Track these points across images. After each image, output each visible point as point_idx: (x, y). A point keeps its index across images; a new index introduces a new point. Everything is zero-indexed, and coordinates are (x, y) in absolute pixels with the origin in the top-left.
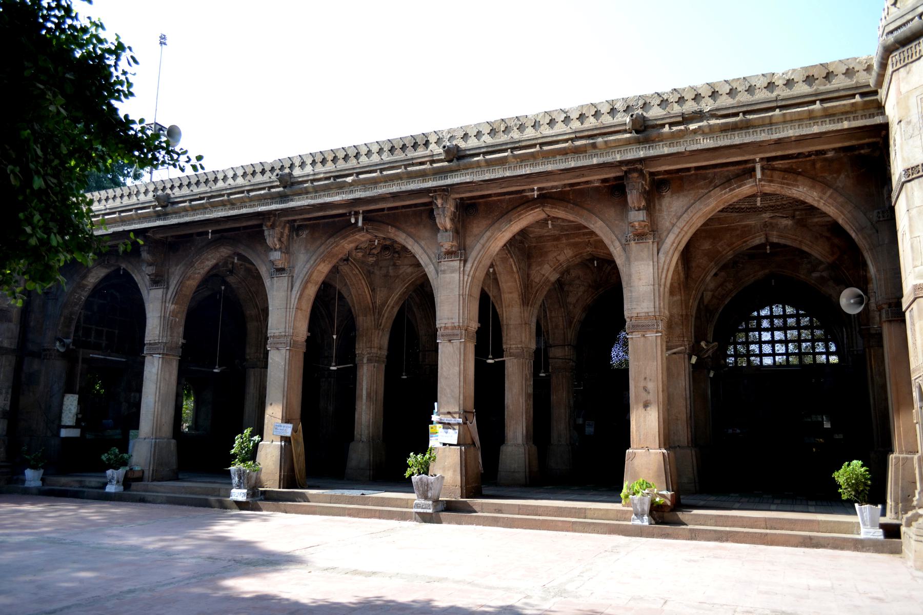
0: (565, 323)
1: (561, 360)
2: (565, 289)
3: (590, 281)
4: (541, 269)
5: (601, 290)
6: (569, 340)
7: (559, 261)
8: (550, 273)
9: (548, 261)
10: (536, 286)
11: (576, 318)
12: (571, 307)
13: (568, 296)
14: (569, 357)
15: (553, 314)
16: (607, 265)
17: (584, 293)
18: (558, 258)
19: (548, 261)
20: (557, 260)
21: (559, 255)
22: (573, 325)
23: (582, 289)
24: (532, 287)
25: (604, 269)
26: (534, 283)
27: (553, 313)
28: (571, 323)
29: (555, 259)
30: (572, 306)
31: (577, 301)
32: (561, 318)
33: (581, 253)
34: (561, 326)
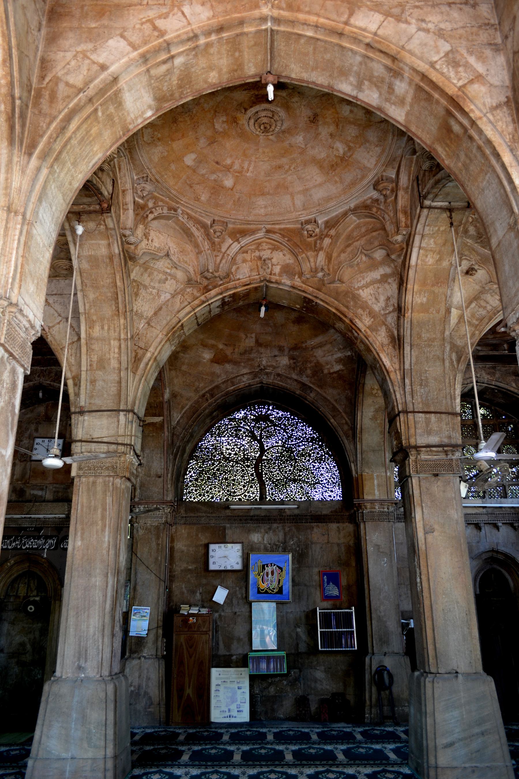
0: (124, 358)
1: (104, 448)
2: (133, 275)
3: (191, 269)
4: (95, 50)
5: (213, 292)
6: (130, 399)
7: (162, 33)
8: (127, 67)
9: (125, 29)
10: (69, 98)
11: (151, 349)
12: (142, 325)
13: (137, 294)
14: (127, 441)
15: (97, 332)
16: (231, 241)
17: (173, 296)
18: (161, 23)
19: (125, 29)
20: (155, 28)
21: (165, 16)
22: (142, 366)
23: (170, 286)
24: (53, 98)
25: (223, 250)
26: (61, 86)
27: (97, 328)
28: (137, 360)
29: (147, 27)
30: (143, 322)
31: (155, 314)
32: (114, 343)
33: (241, 23)
34: (114, 363)
